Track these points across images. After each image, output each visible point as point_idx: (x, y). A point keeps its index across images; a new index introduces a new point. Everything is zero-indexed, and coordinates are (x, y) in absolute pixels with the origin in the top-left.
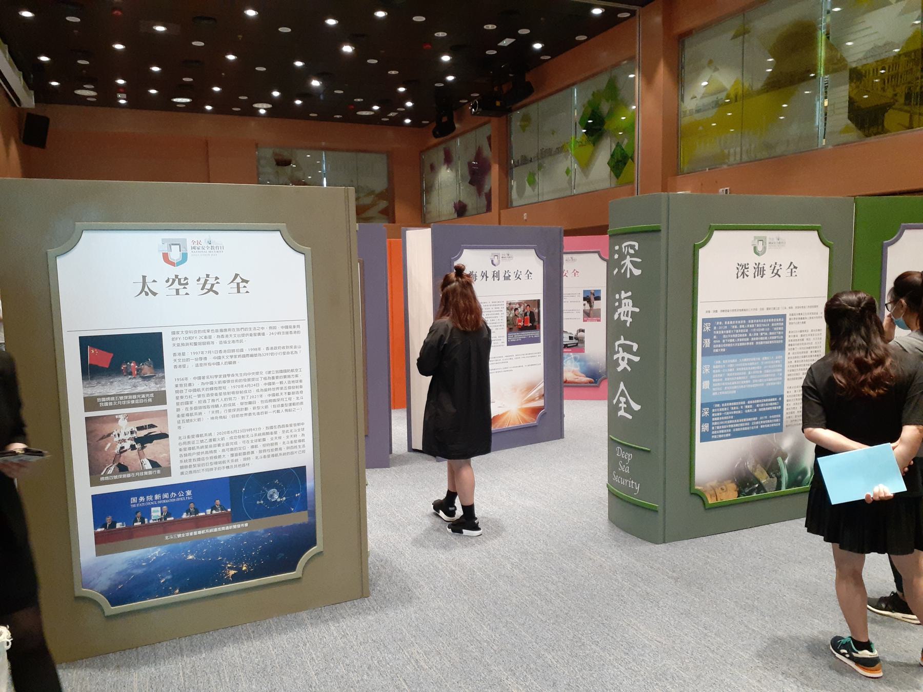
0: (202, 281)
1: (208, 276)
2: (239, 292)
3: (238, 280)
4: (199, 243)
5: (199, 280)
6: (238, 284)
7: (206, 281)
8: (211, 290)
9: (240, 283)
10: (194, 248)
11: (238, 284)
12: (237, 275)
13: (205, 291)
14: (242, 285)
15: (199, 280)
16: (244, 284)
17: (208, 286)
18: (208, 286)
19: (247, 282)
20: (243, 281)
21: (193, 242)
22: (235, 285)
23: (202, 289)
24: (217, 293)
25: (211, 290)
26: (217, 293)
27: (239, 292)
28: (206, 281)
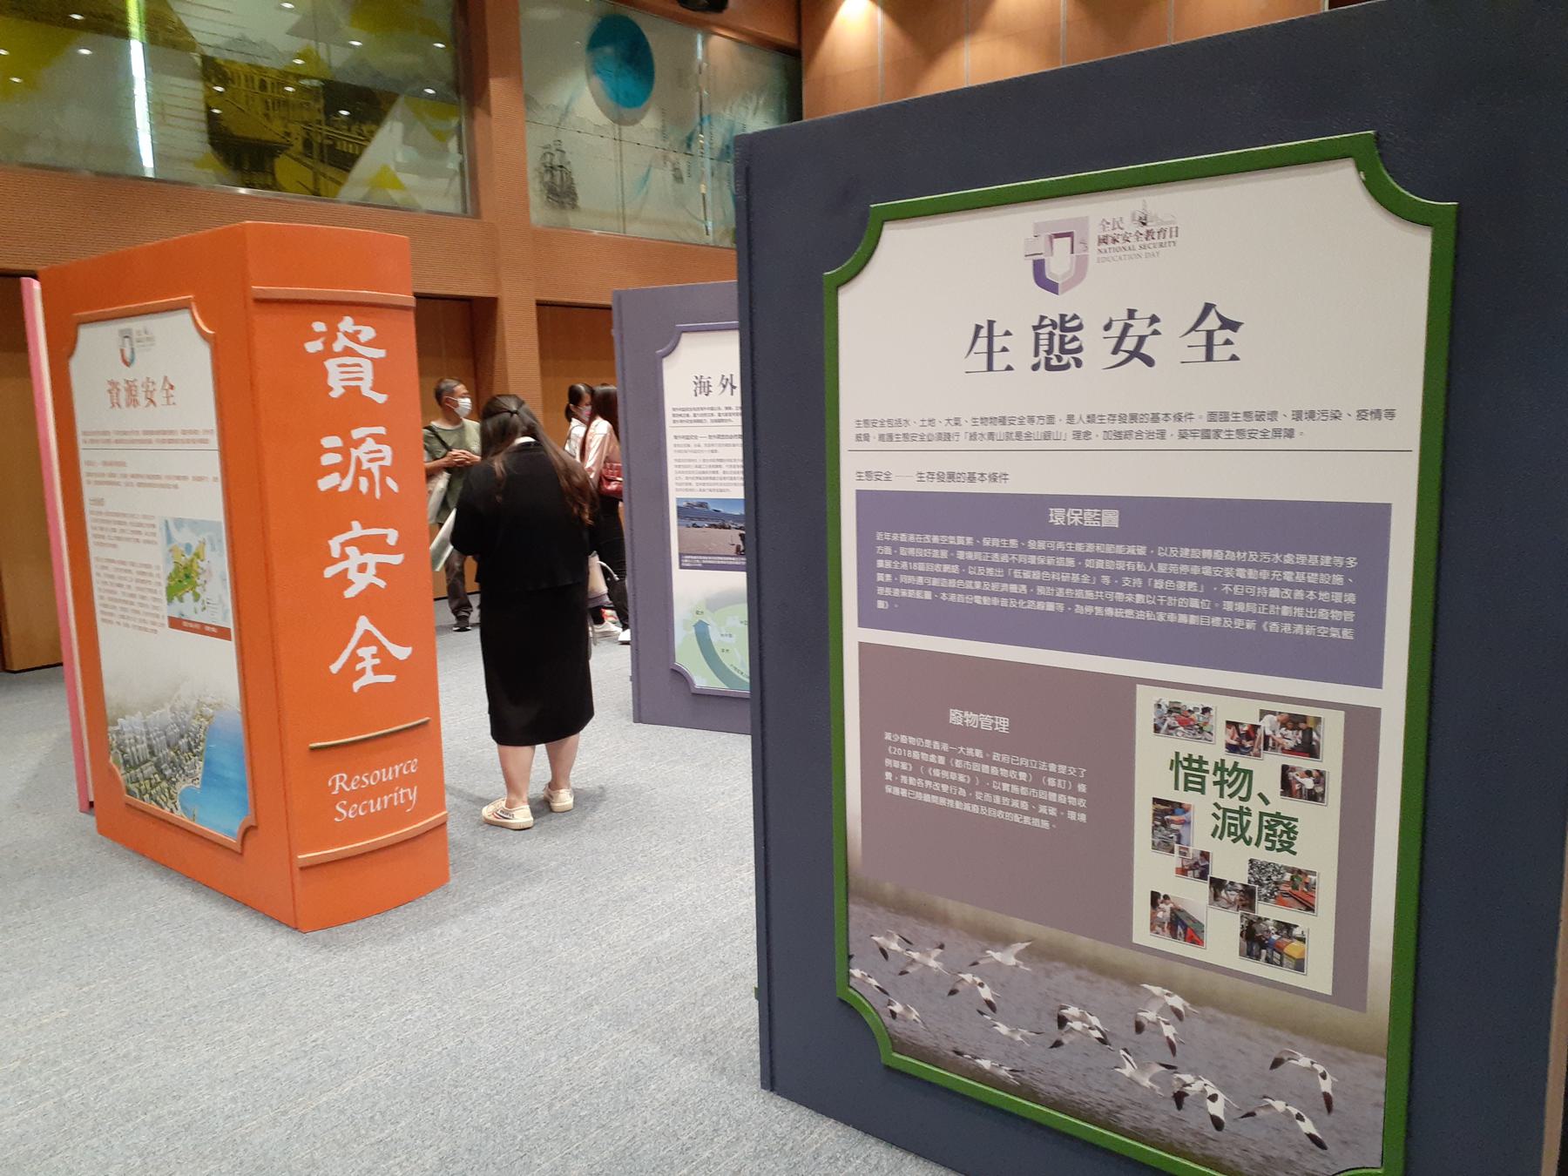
0: (1117, 330)
1: (1131, 314)
2: (1209, 357)
3: (1212, 322)
4: (1117, 224)
5: (1107, 327)
6: (1210, 334)
7: (1127, 327)
8: (1135, 353)
9: (1216, 329)
10: (1103, 241)
11: (1210, 334)
12: (1208, 308)
13: (1122, 356)
14: (1219, 337)
15: (1107, 327)
16: (1228, 334)
17: (1129, 344)
18: (1129, 344)
19: (1233, 326)
20: (1229, 325)
21: (1105, 223)
22: (1200, 338)
23: (1115, 351)
24: (1149, 362)
25: (1135, 353)
26: (1149, 362)
27: (1209, 357)
28: (1127, 327)
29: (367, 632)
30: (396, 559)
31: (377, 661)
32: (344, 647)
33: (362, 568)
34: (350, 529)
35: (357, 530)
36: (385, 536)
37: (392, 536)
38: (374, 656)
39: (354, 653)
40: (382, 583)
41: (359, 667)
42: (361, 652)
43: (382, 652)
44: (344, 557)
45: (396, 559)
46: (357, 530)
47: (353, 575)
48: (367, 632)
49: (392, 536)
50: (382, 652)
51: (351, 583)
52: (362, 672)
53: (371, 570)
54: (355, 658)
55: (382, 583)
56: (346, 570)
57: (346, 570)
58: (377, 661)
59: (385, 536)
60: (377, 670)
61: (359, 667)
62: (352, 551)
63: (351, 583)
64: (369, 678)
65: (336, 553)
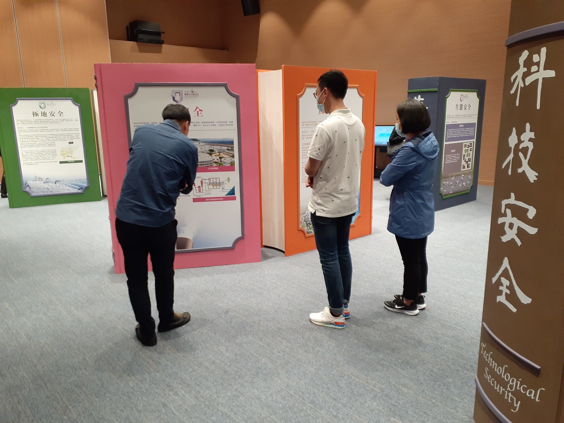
29: (506, 269)
30: (532, 231)
31: (508, 292)
32: (497, 272)
33: (511, 226)
34: (509, 197)
35: (512, 200)
36: (527, 210)
37: (532, 213)
38: (507, 287)
39: (499, 279)
40: (519, 243)
41: (501, 288)
42: (503, 280)
43: (511, 287)
44: (505, 215)
45: (532, 231)
46: (512, 200)
47: (506, 228)
48: (506, 269)
49: (532, 213)
50: (511, 287)
51: (504, 233)
52: (500, 293)
53: (515, 230)
54: (499, 283)
55: (519, 243)
56: (504, 224)
57: (504, 224)
58: (508, 292)
59: (527, 210)
60: (508, 297)
61: (501, 288)
62: (509, 212)
63: (504, 233)
64: (501, 299)
65: (503, 212)
